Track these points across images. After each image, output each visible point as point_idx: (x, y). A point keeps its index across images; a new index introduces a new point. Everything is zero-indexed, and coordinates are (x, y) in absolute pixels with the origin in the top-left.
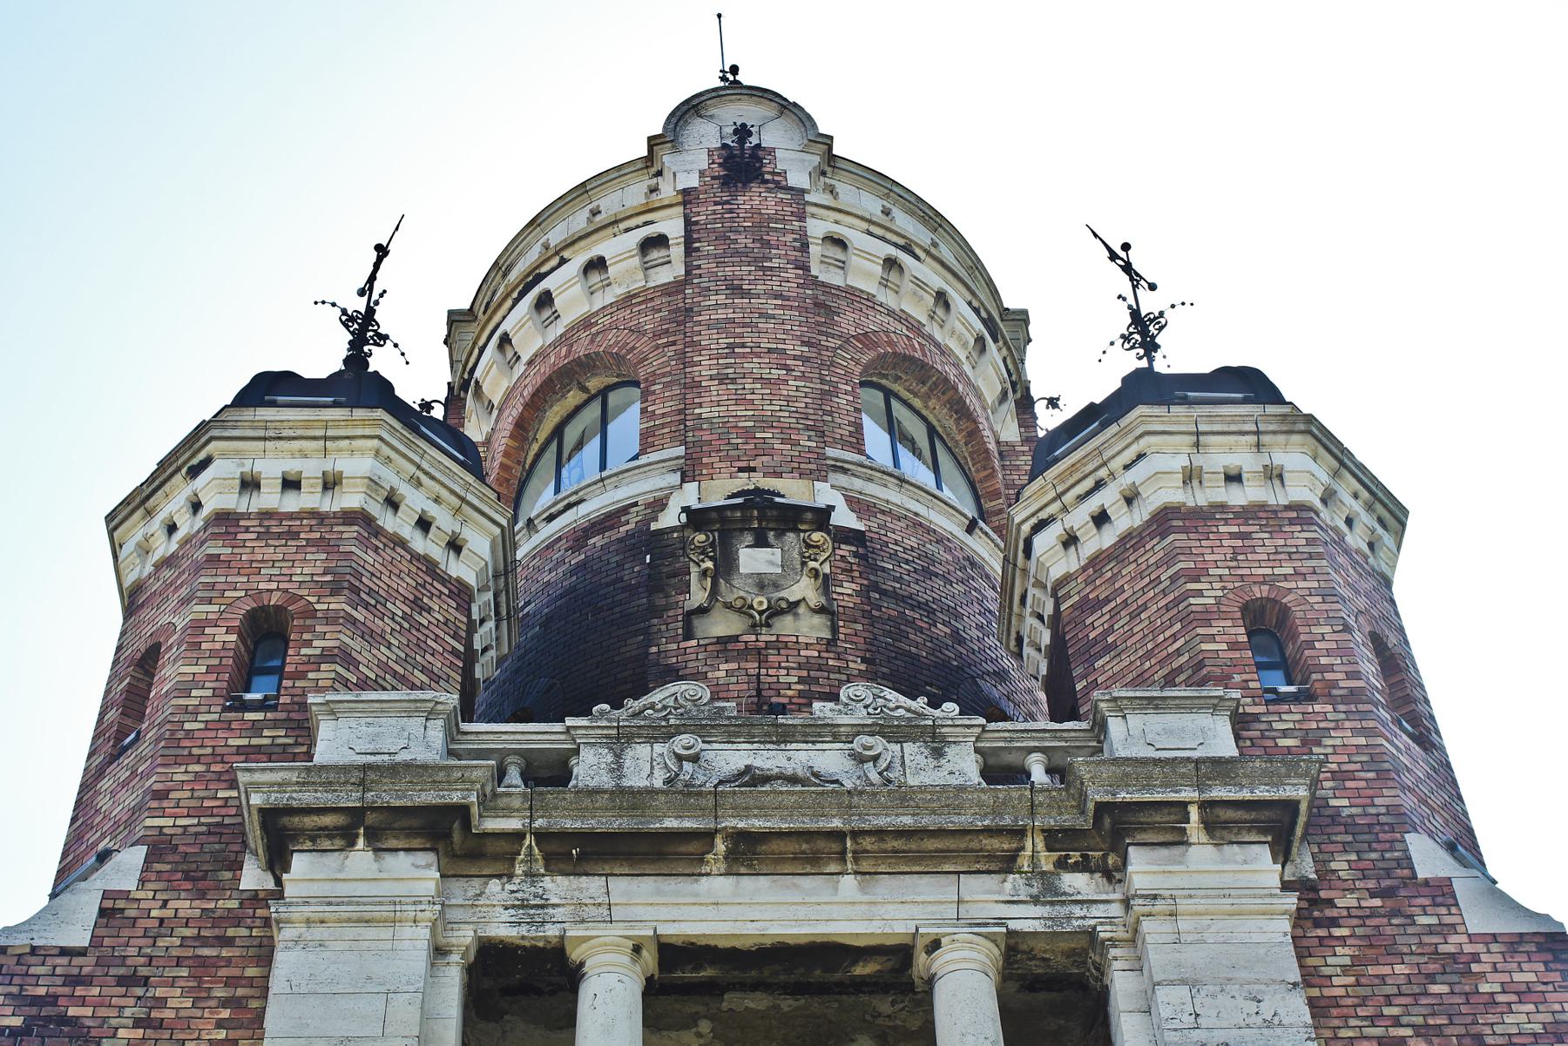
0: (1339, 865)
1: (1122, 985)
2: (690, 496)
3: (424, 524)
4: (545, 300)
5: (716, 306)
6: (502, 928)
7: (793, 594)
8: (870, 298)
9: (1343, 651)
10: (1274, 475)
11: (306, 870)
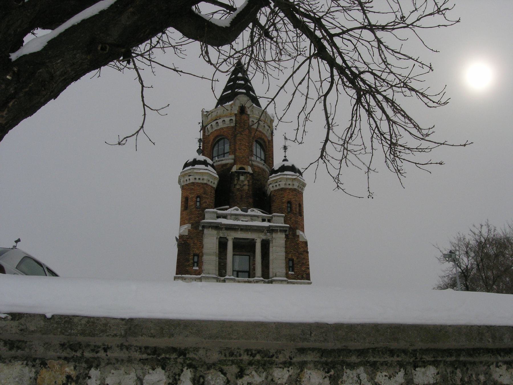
0: (290, 233)
1: (271, 245)
2: (234, 169)
4: (217, 123)
5: (239, 137)
6: (222, 235)
7: (245, 183)
9: (296, 208)
11: (206, 231)
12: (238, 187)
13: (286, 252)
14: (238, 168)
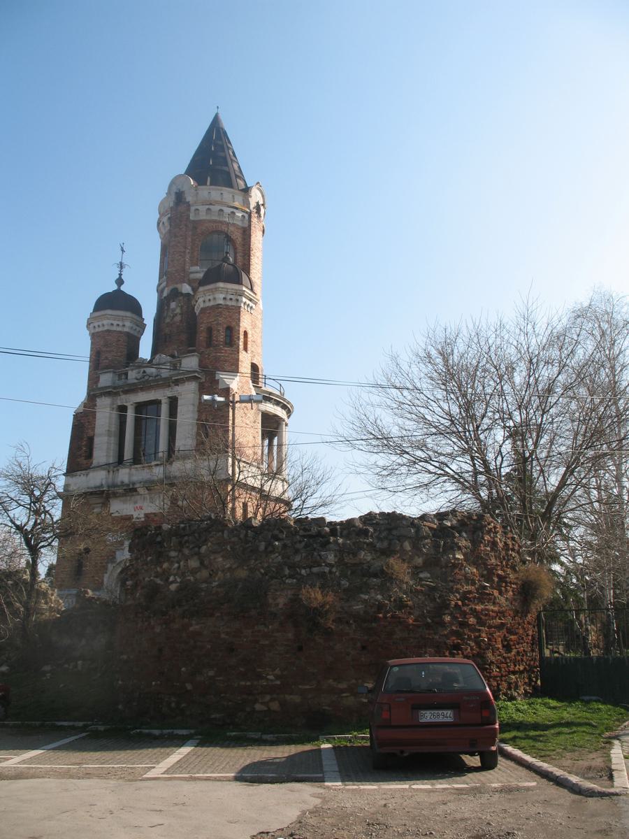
3: (118, 325)
8: (204, 220)
10: (215, 299)
12: (168, 320)
13: (199, 411)
14: (169, 291)
